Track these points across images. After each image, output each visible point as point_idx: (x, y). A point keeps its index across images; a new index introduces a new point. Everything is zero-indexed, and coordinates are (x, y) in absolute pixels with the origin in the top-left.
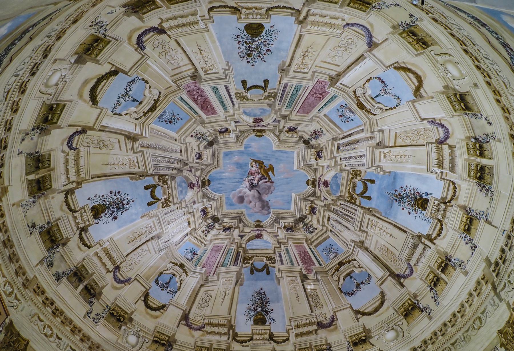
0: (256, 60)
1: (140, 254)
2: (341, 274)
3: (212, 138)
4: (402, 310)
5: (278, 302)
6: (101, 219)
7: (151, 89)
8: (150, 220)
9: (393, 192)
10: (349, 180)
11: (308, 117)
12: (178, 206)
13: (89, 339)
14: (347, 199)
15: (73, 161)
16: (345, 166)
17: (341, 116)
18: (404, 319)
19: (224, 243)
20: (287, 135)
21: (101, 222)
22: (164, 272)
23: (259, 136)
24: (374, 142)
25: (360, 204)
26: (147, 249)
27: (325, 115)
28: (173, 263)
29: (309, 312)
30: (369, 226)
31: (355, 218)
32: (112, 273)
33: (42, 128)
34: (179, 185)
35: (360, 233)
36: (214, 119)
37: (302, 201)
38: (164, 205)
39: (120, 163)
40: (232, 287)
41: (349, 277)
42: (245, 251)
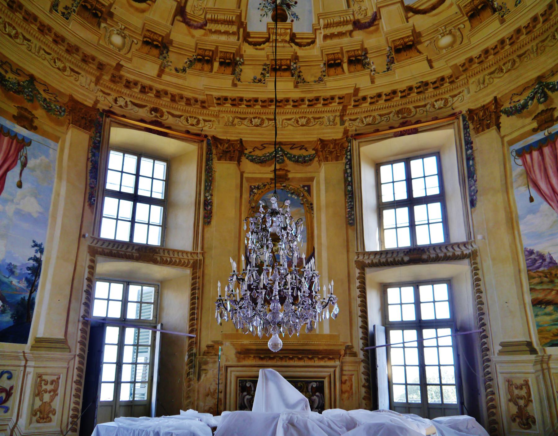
4: (468, 9)
18: (468, 22)
29: (345, 7)
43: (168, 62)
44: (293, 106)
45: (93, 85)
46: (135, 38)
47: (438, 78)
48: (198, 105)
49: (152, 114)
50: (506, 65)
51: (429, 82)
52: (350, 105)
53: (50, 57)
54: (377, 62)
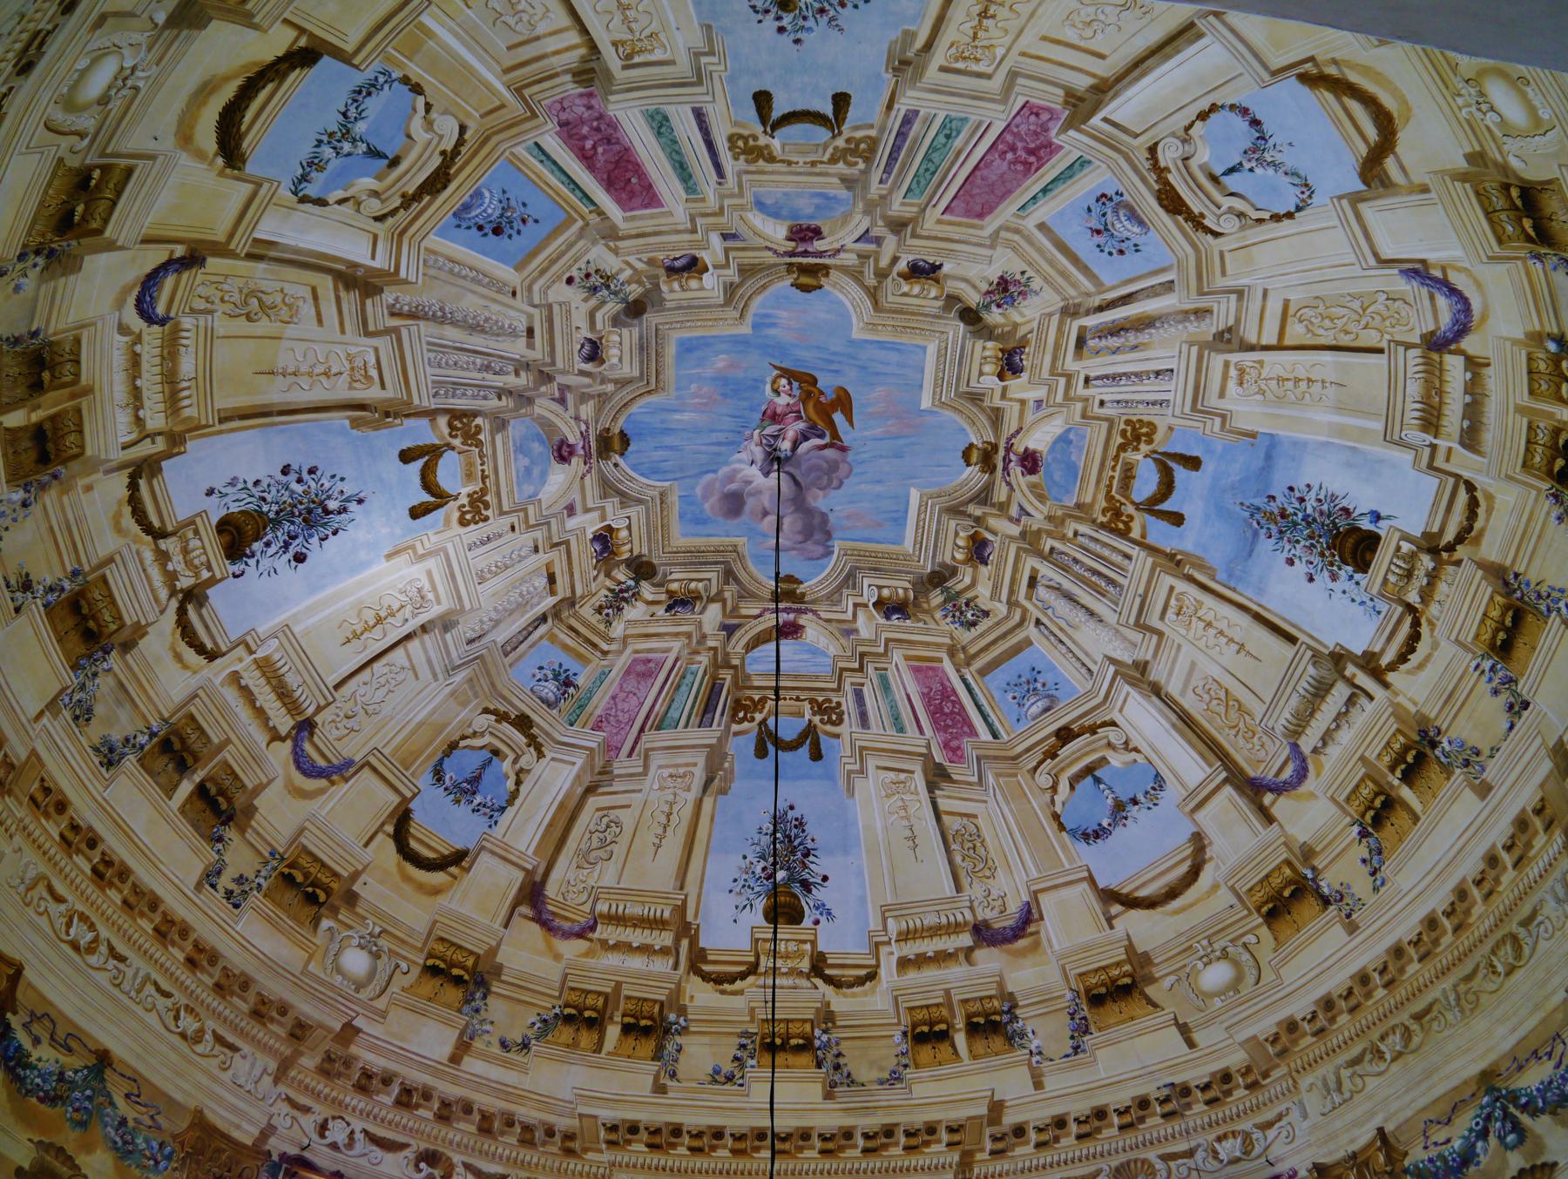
0: (810, 23)
1: (382, 680)
2: (1062, 770)
3: (640, 290)
5: (846, 851)
6: (252, 562)
7: (434, 115)
8: (415, 567)
9: (1260, 501)
10: (1112, 451)
11: (982, 228)
13: (214, 957)
14: (1101, 519)
15: (158, 360)
16: (1102, 403)
17: (1098, 232)
18: (1265, 929)
19: (668, 650)
20: (906, 288)
21: (251, 571)
22: (462, 743)
23: (806, 289)
24: (1208, 328)
25: (1143, 536)
26: (407, 664)
27: (1042, 227)
28: (495, 712)
29: (948, 888)
30: (1170, 615)
31: (1125, 582)
32: (289, 743)
33: (52, 252)
34: (521, 449)
35: (1136, 636)
37: (945, 518)
38: (468, 517)
40: (691, 796)
41: (1089, 779)
43: (482, 1021)
44: (822, 1152)
45: (267, 1080)
46: (405, 958)
47: (1213, 1074)
48: (554, 1144)
49: (420, 1171)
50: (1390, 1040)
51: (1193, 1084)
52: (982, 1150)
53: (169, 1002)
54: (1045, 1030)
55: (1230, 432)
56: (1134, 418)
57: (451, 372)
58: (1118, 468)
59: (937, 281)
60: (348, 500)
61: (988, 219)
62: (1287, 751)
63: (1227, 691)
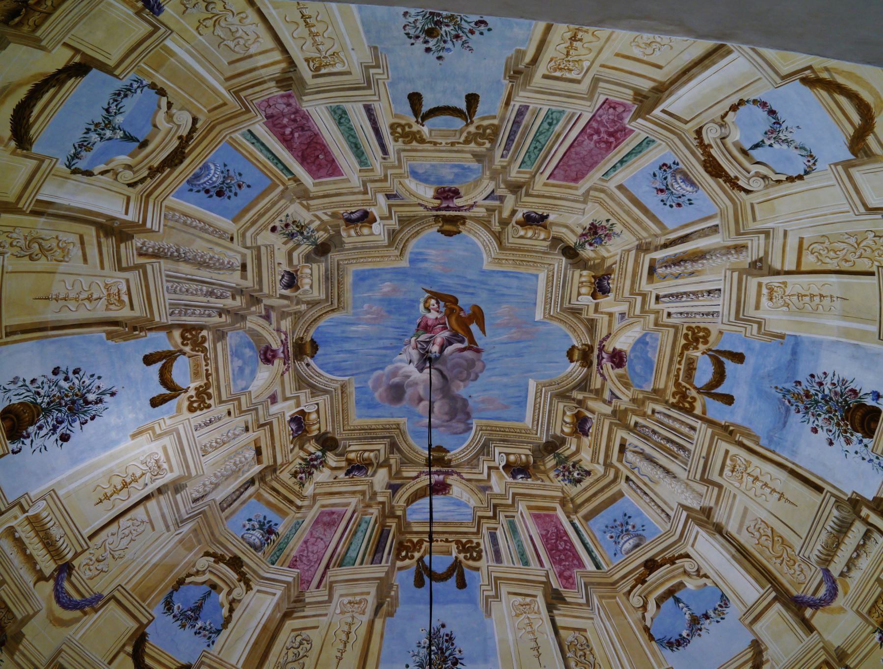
0: (449, 45)
1: (127, 532)
2: (650, 592)
3: (326, 236)
5: (486, 660)
6: (27, 441)
7: (174, 111)
8: (154, 444)
9: (789, 386)
10: (678, 350)
11: (577, 189)
12: (231, 407)
14: (672, 400)
16: (669, 315)
17: (662, 191)
19: (348, 505)
20: (522, 233)
21: (27, 448)
22: (188, 580)
23: (449, 234)
24: (745, 259)
25: (704, 413)
26: (146, 519)
27: (621, 187)
28: (214, 555)
30: (727, 471)
32: (52, 582)
34: (236, 354)
35: (702, 489)
36: (334, 187)
37: (555, 401)
38: (195, 405)
39: (82, 297)
40: (366, 618)
41: (671, 600)
42: (404, 526)
55: (765, 334)
56: (694, 325)
57: (183, 297)
58: (683, 362)
59: (545, 227)
60: (103, 393)
61: (581, 182)
62: (821, 575)
63: (772, 529)
